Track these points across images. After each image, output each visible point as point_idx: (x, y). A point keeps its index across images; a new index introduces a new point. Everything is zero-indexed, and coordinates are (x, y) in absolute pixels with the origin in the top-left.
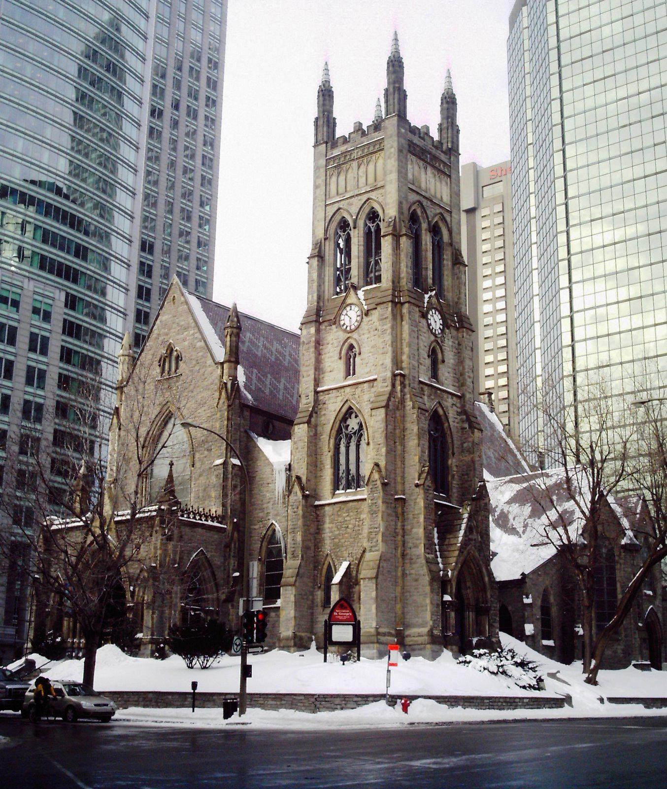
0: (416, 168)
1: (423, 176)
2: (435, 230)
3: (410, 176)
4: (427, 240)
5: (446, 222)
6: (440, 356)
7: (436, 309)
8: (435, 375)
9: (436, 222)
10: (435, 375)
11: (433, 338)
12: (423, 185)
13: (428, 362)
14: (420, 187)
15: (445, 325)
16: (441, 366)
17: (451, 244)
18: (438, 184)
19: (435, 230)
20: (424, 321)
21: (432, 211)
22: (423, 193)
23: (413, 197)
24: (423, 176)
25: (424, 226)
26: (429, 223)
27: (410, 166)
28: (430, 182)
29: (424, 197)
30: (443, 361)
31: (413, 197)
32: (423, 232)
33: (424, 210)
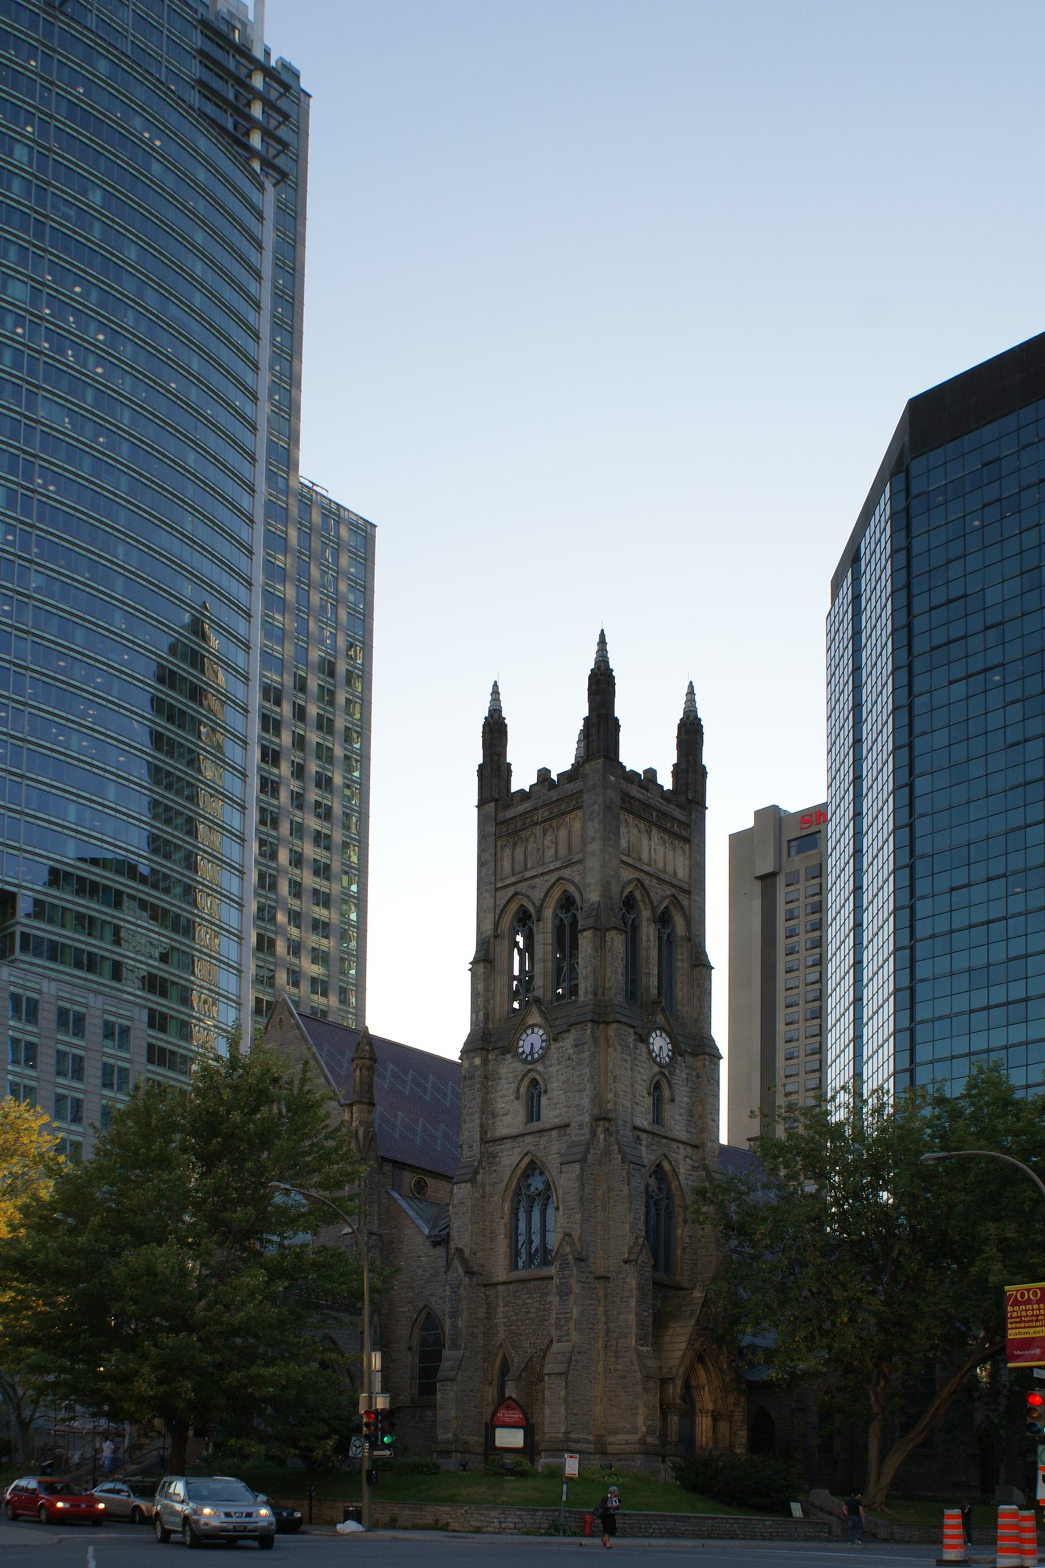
0: (635, 832)
1: (645, 842)
2: (663, 920)
3: (624, 844)
4: (648, 933)
5: (682, 907)
6: (667, 1093)
7: (662, 1029)
8: (658, 1117)
9: (666, 908)
10: (658, 1117)
11: (656, 1069)
12: (645, 856)
13: (649, 1101)
14: (640, 860)
15: (677, 1051)
16: (667, 1106)
17: (689, 939)
18: (670, 854)
19: (663, 920)
20: (642, 1046)
21: (658, 892)
22: (645, 868)
23: (628, 874)
24: (645, 842)
25: (646, 914)
26: (654, 910)
27: (623, 830)
28: (656, 851)
29: (647, 873)
30: (672, 1100)
31: (628, 874)
32: (645, 923)
33: (646, 892)
